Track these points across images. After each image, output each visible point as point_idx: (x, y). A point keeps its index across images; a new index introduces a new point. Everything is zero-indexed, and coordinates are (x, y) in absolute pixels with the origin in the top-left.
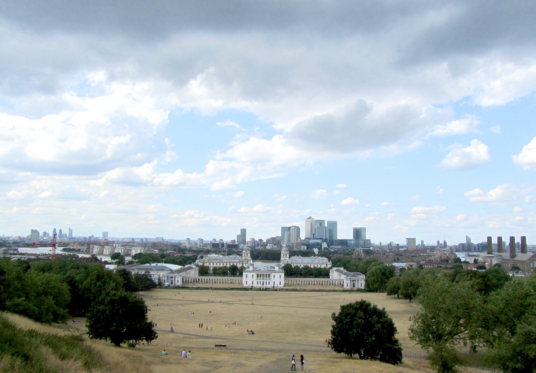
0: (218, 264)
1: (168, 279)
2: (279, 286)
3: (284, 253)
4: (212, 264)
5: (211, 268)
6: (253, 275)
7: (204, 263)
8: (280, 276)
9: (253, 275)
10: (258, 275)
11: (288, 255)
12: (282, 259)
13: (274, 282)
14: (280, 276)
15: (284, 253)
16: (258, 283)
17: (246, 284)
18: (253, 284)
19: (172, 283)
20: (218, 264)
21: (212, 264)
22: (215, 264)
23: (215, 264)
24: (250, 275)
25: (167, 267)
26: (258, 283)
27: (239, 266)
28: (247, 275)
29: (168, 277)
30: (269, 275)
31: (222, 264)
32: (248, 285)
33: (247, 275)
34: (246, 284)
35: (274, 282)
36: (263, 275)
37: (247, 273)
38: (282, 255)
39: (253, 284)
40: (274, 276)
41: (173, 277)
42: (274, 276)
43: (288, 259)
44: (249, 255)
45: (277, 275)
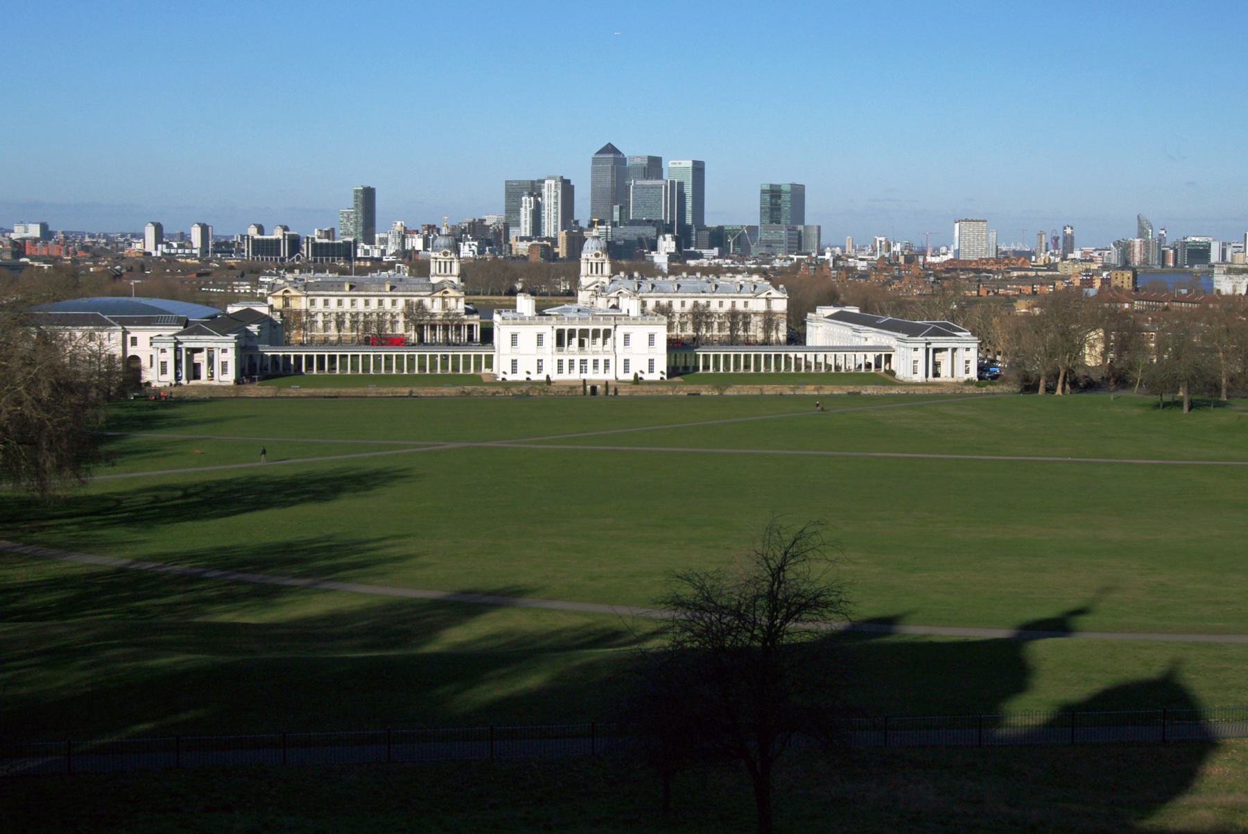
0: (347, 301)
1: (177, 363)
2: (647, 377)
3: (594, 260)
4: (319, 301)
5: (320, 318)
6: (540, 337)
7: (286, 300)
8: (651, 337)
9: (540, 337)
10: (560, 334)
11: (607, 267)
12: (584, 281)
13: (626, 362)
14: (651, 337)
15: (594, 260)
16: (560, 370)
17: (514, 371)
18: (540, 369)
19: (197, 377)
20: (347, 301)
21: (319, 301)
22: (333, 301)
23: (333, 301)
24: (527, 334)
25: (163, 312)
26: (560, 370)
27: (435, 306)
28: (514, 337)
29: (177, 350)
30: (607, 333)
31: (361, 301)
32: (521, 376)
33: (514, 337)
34: (514, 371)
35: (626, 362)
36: (584, 333)
37: (514, 329)
38: (584, 268)
39: (540, 369)
40: (627, 337)
41: (200, 350)
42: (627, 337)
43: (607, 280)
44: (456, 270)
45: (639, 334)
